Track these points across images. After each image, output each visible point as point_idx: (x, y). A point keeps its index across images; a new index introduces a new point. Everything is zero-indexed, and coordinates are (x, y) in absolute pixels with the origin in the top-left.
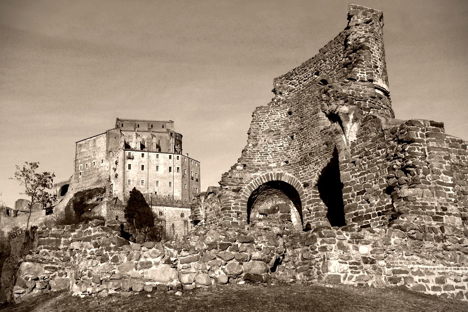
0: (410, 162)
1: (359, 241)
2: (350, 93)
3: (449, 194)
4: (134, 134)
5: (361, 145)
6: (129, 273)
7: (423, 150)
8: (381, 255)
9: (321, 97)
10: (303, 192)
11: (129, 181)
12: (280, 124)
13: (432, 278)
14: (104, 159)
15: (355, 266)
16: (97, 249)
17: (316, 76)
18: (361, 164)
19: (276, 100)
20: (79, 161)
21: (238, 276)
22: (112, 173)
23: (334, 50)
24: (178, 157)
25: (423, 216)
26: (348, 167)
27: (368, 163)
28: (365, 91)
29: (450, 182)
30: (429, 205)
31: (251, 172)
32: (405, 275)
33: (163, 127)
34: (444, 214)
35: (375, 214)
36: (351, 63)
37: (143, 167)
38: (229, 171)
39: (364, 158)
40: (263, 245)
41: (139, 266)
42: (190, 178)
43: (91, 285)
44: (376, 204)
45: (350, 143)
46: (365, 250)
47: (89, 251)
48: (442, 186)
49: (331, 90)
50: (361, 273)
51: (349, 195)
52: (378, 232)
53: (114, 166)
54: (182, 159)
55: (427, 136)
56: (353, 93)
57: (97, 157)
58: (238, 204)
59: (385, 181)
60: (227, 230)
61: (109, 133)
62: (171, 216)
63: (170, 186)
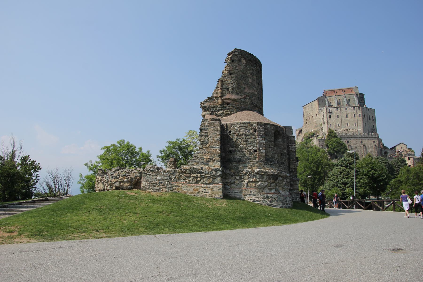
4: (334, 98)
7: (206, 133)
14: (318, 114)
24: (359, 108)
37: (338, 116)
53: (322, 117)
54: (362, 109)
63: (355, 125)
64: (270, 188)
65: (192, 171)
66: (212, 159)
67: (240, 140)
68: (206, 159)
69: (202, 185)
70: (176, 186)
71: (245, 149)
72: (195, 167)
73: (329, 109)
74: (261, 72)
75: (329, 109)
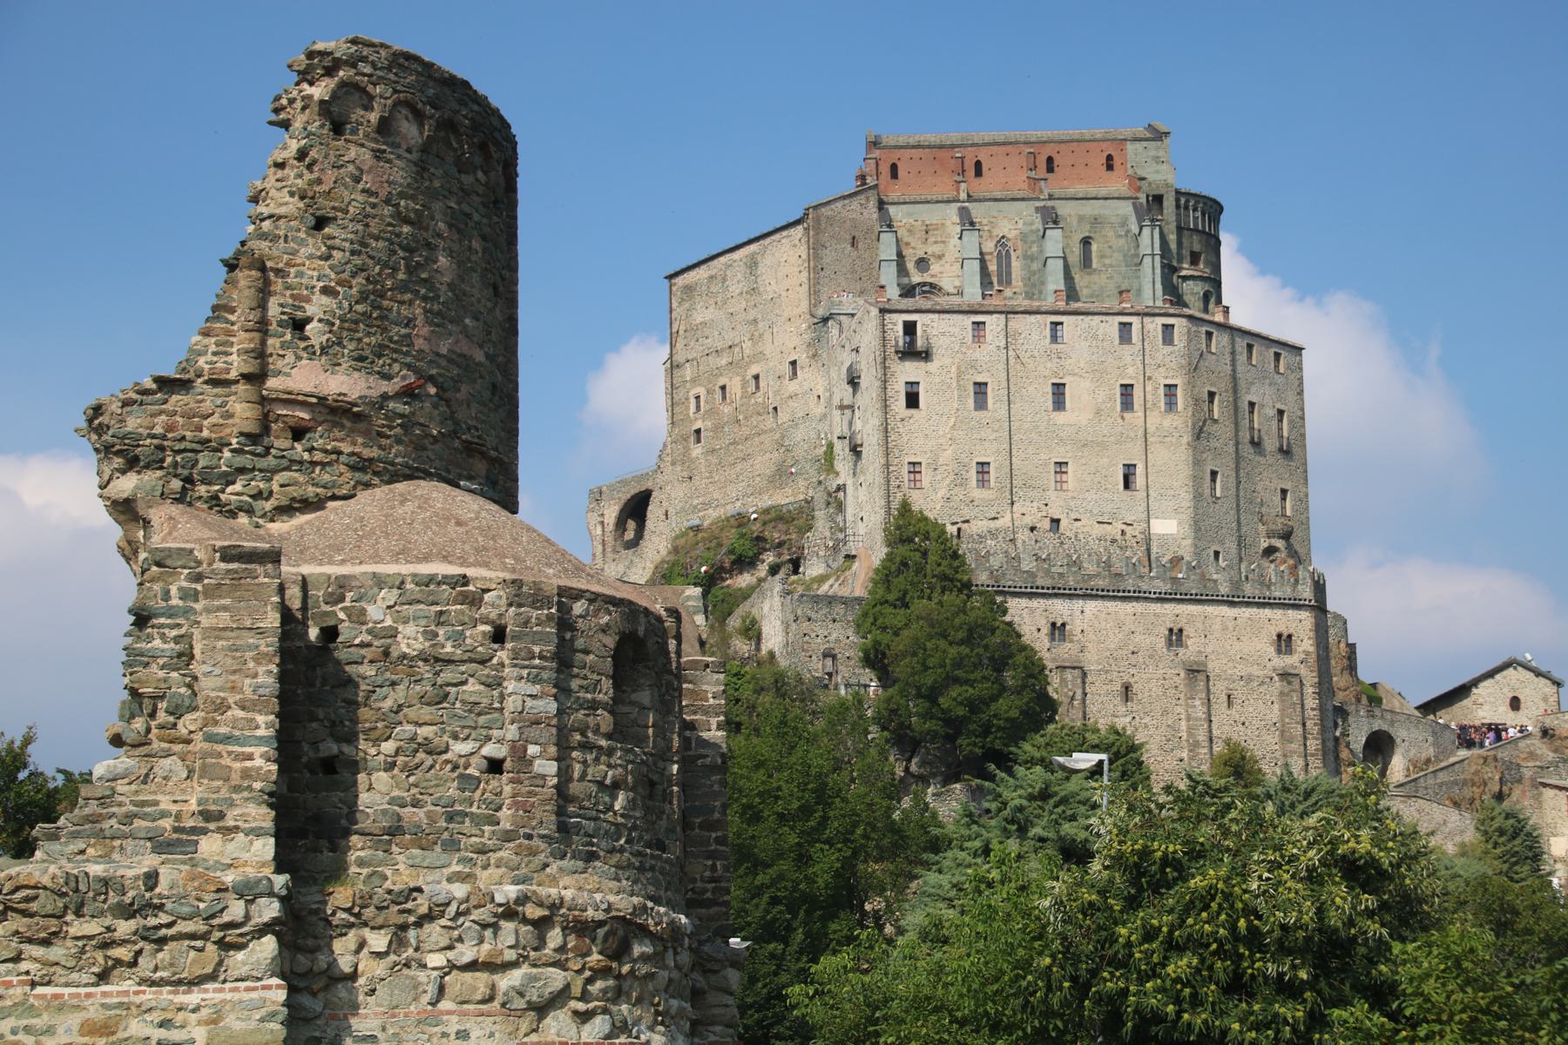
2: (158, 430)
7: (177, 640)
11: (915, 467)
13: (74, 1020)
14: (803, 358)
20: (688, 372)
30: (165, 804)
34: (205, 832)
48: (219, 748)
57: (768, 349)
62: (1114, 640)
64: (581, 1006)
65: (75, 897)
66: (221, 816)
67: (400, 694)
68: (178, 817)
69: (149, 995)
71: (430, 753)
72: (96, 869)
74: (513, 205)
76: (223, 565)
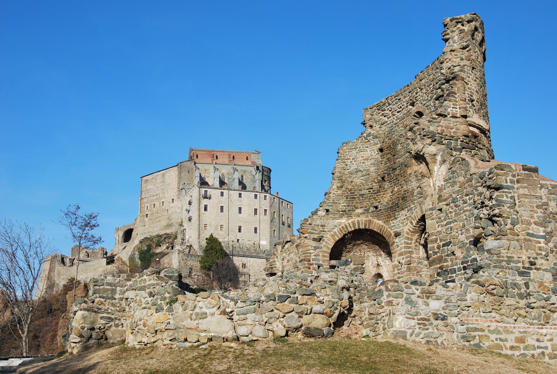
0: (497, 211)
1: (429, 296)
3: (540, 247)
5: (448, 191)
6: (183, 324)
8: (453, 312)
9: (406, 135)
10: (394, 243)
12: (369, 163)
13: (512, 337)
15: (424, 322)
16: (152, 298)
17: (411, 107)
18: (448, 212)
19: (365, 135)
20: (145, 200)
21: (297, 329)
22: (185, 216)
23: (431, 77)
24: (265, 196)
25: (507, 271)
26: (435, 216)
27: (455, 211)
28: (457, 129)
29: (542, 234)
30: (516, 259)
31: (334, 219)
32: (480, 333)
33: (247, 159)
34: (532, 269)
35: (460, 268)
36: (442, 96)
37: (222, 208)
38: (310, 217)
39: (451, 205)
40: (326, 298)
41: (194, 317)
42: (281, 222)
43: (146, 335)
44: (461, 257)
45: (437, 188)
46: (435, 305)
47: (144, 301)
48: (531, 238)
49: (417, 127)
50: (430, 330)
51: (434, 247)
52: (452, 287)
53: (188, 206)
54: (271, 199)
55: (518, 182)
56: (443, 131)
57: (166, 195)
58: (318, 255)
59: (471, 232)
60: (288, 281)
61: (181, 166)
66: (535, 264)
70: (476, 329)
73: (206, 191)
75: (206, 191)
76: (523, 172)
